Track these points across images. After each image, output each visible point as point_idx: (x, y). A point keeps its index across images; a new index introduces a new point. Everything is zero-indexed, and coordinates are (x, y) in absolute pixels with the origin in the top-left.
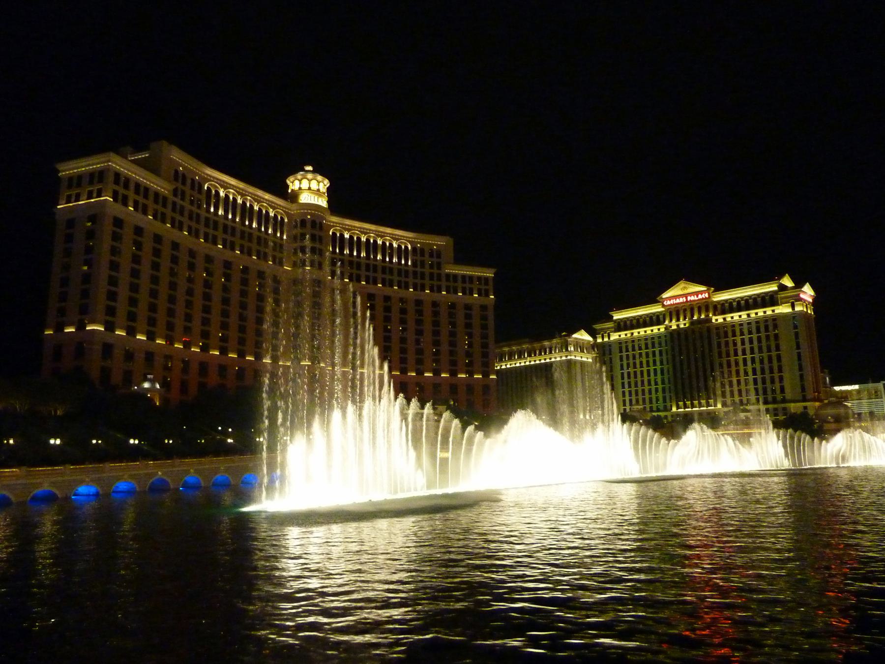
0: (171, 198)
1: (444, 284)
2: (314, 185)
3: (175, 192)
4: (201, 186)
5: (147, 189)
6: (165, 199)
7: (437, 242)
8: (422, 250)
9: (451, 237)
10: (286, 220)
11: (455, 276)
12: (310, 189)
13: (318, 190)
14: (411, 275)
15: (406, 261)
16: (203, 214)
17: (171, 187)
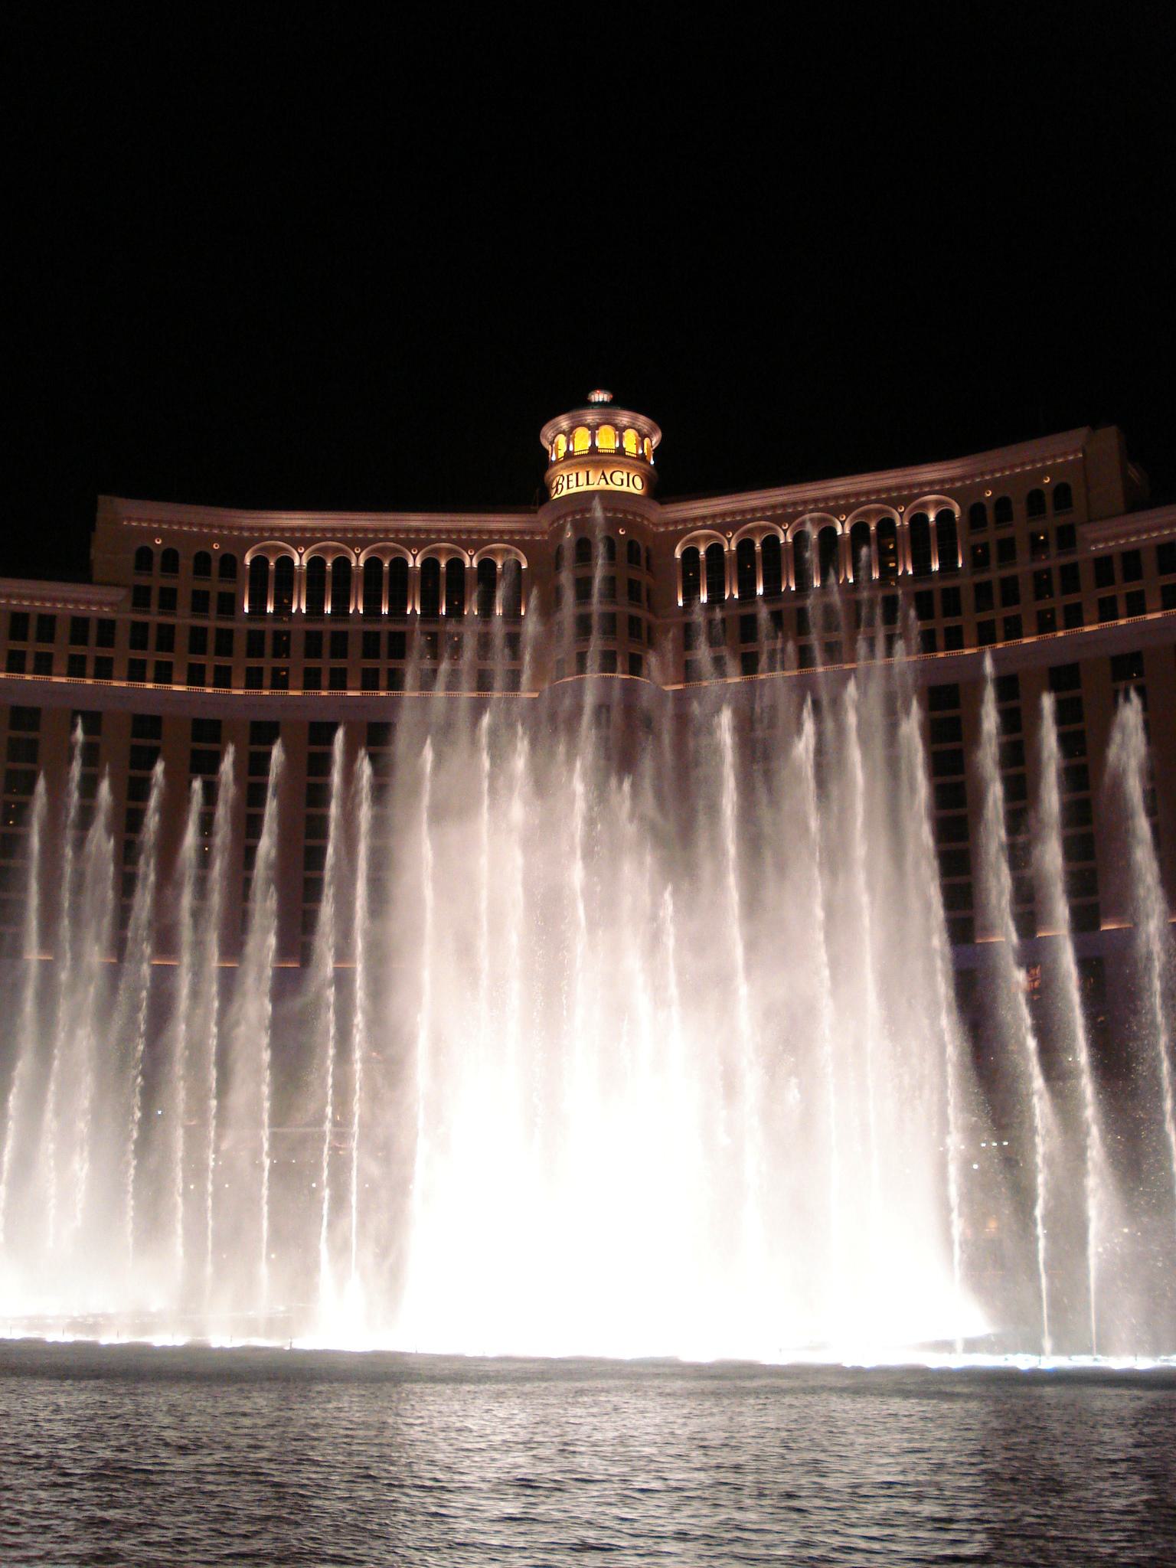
0: (125, 616)
1: (1089, 595)
2: (582, 442)
3: (140, 598)
4: (229, 564)
5: (47, 624)
6: (107, 629)
7: (1047, 458)
8: (1003, 506)
9: (1082, 425)
10: (524, 566)
11: (1132, 560)
12: (597, 453)
13: (593, 449)
14: (968, 600)
15: (948, 562)
16: (240, 628)
17: (119, 594)
